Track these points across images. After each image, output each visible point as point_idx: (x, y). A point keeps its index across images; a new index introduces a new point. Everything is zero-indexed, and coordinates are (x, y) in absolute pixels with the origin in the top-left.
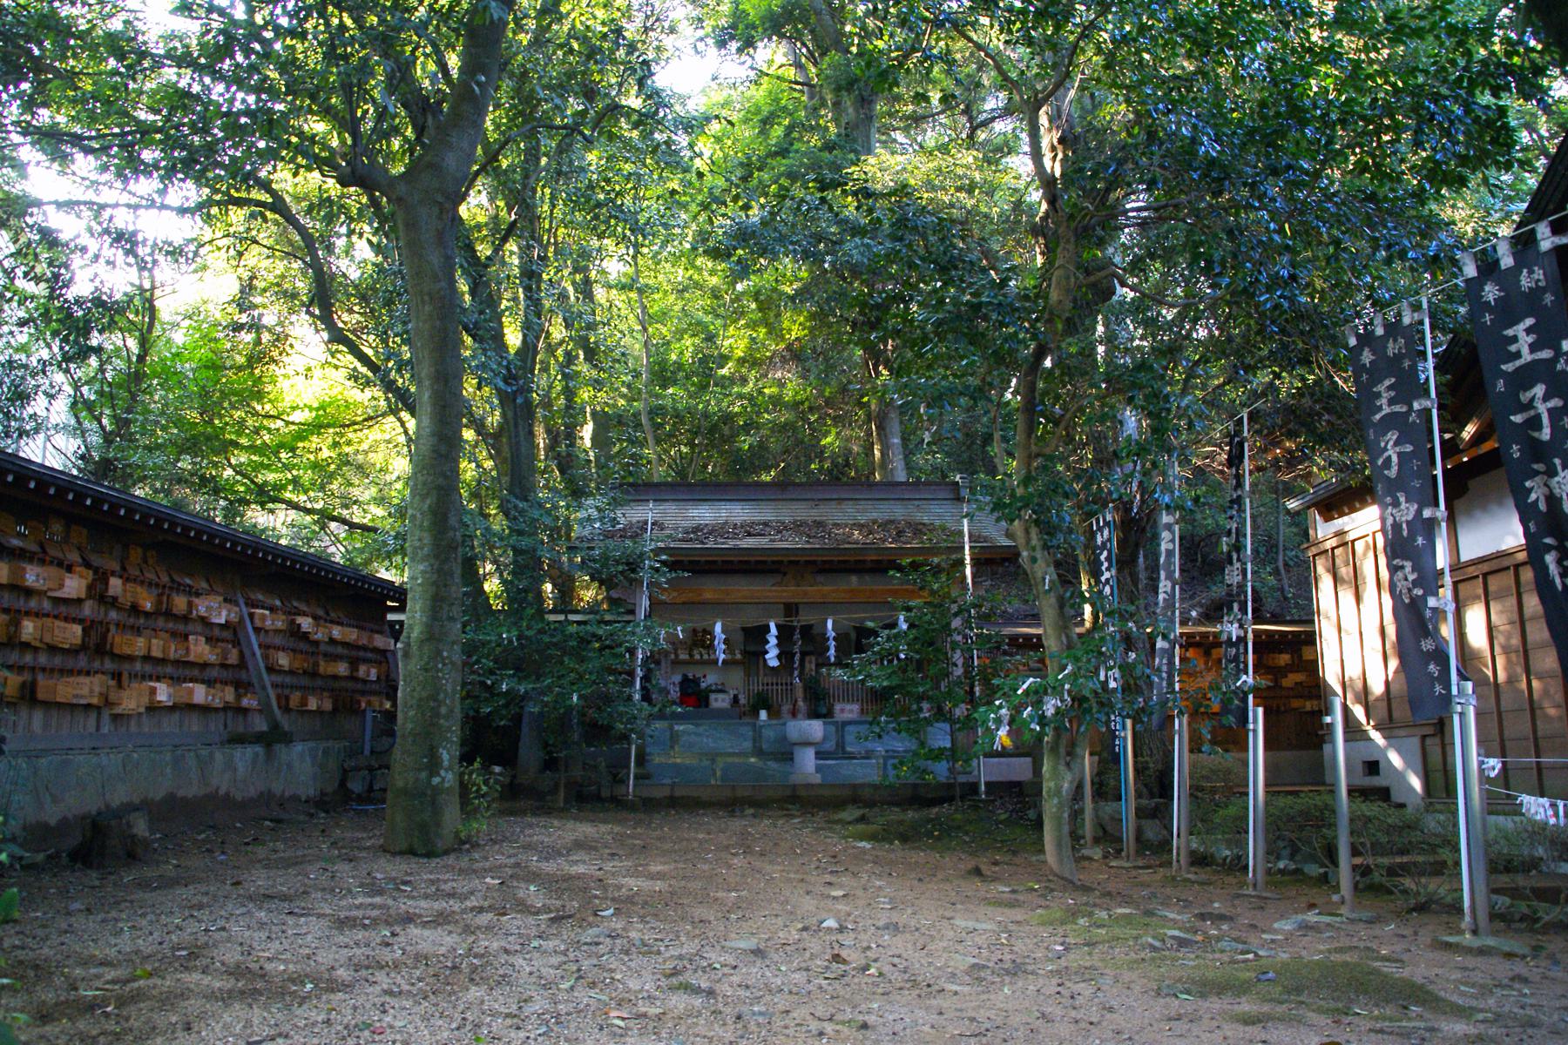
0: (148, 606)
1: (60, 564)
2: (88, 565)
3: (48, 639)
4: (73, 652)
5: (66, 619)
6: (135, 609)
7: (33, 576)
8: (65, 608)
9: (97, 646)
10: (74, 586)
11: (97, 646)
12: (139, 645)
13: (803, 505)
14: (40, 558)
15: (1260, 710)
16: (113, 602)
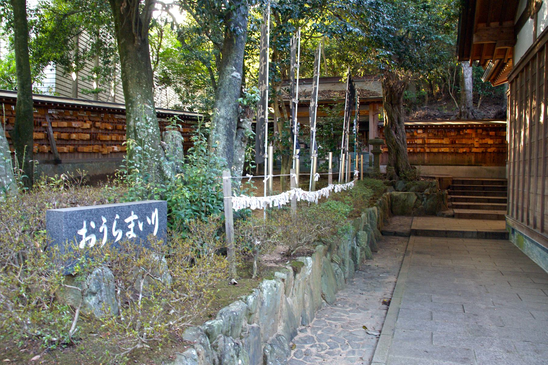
0: (110, 128)
1: (82, 121)
2: (90, 120)
3: (80, 138)
4: (87, 140)
5: (85, 133)
6: (106, 129)
7: (74, 124)
8: (85, 131)
9: (94, 139)
10: (87, 125)
11: (94, 139)
12: (108, 138)
13: (330, 85)
14: (77, 119)
15: (271, 148)
16: (99, 128)
